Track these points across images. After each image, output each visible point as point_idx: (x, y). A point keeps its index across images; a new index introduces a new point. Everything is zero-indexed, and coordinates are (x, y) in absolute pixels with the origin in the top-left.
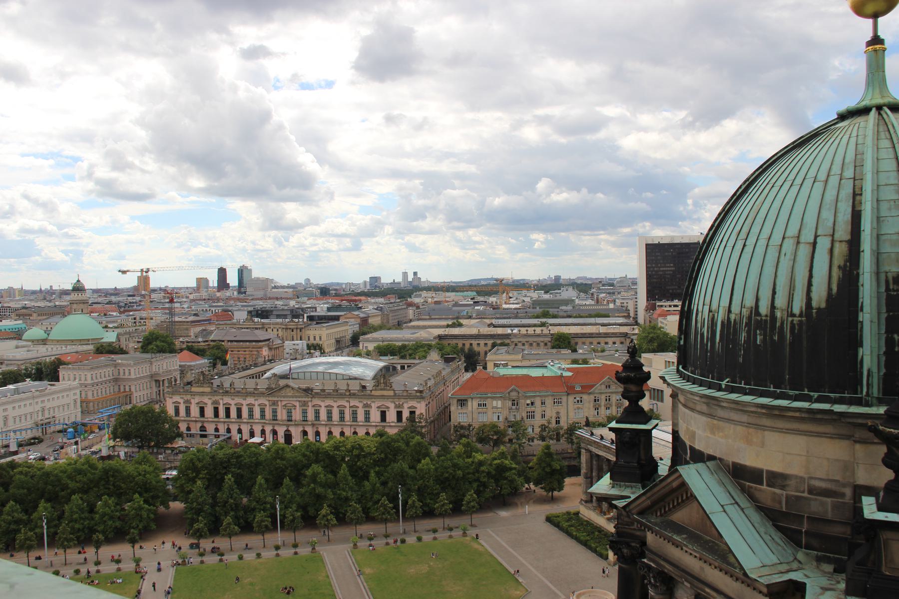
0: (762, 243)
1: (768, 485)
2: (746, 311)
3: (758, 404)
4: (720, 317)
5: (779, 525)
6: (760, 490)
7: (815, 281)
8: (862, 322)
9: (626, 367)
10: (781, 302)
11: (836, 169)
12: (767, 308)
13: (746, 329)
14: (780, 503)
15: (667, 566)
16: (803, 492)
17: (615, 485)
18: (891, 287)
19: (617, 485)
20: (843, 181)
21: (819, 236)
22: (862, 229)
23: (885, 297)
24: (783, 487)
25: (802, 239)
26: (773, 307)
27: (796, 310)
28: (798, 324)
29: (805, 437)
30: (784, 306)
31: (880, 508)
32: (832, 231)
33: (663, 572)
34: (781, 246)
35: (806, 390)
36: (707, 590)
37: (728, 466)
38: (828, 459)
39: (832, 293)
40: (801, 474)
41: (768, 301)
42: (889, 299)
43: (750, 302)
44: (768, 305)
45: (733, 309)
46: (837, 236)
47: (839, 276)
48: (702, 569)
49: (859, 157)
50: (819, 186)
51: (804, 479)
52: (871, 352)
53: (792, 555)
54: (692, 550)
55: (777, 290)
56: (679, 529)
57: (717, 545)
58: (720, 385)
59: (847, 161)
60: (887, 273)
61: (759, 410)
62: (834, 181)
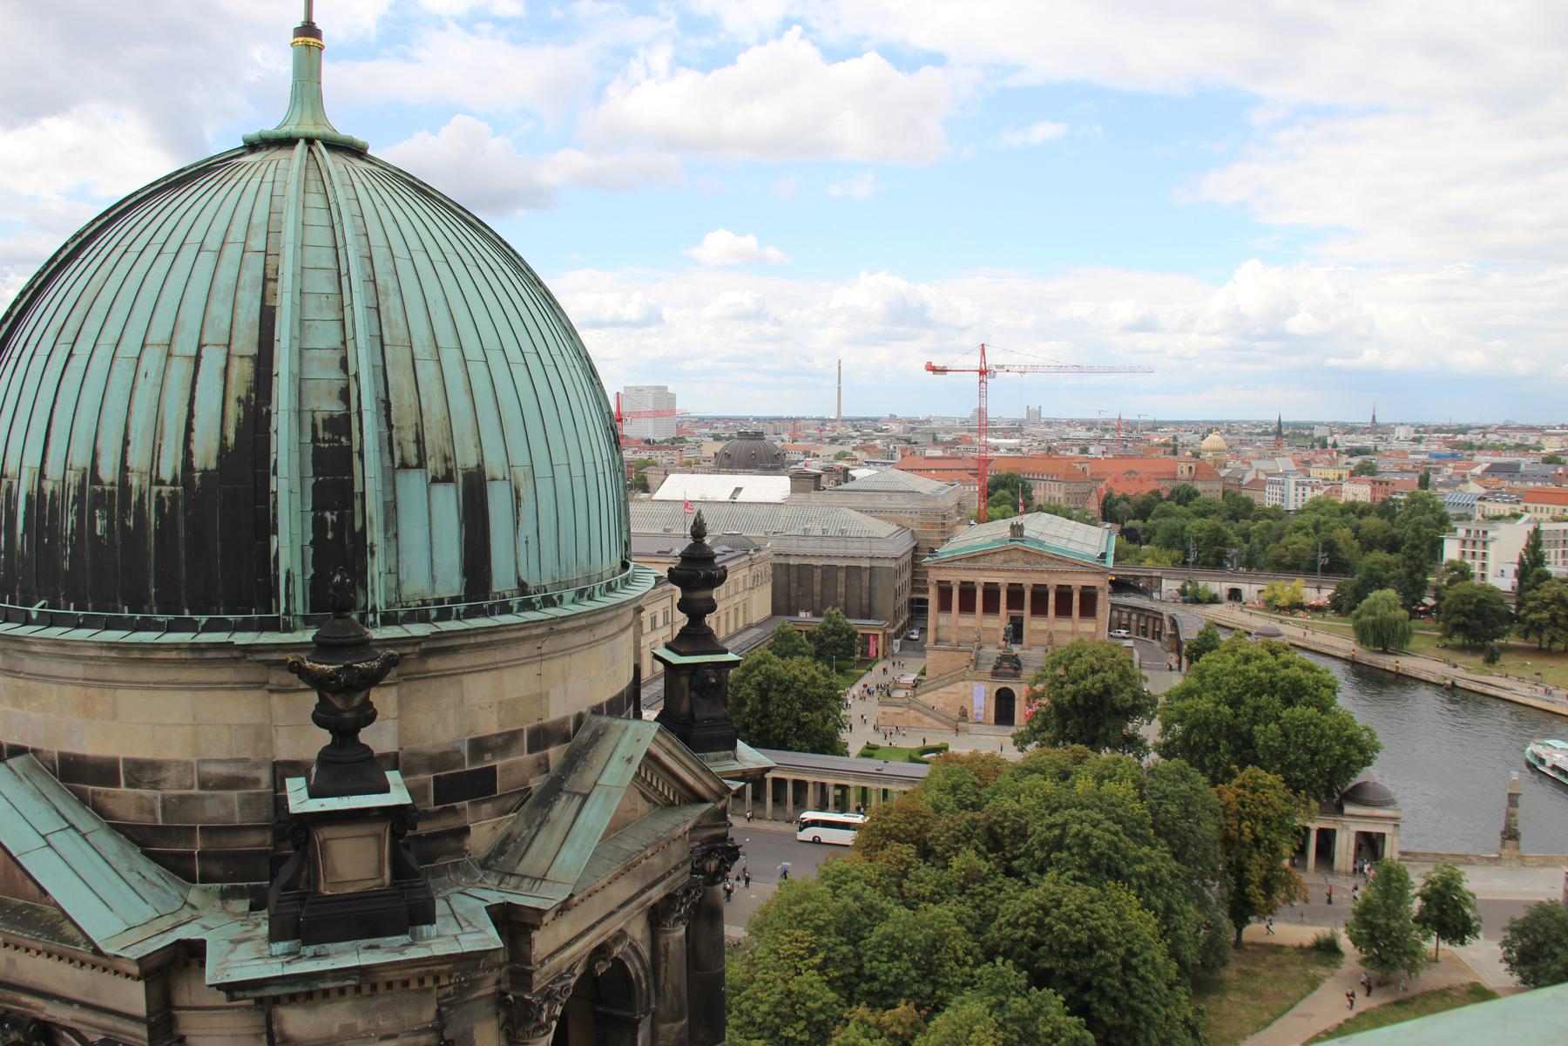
0: (104, 351)
1: (129, 785)
2: (75, 475)
4: (24, 487)
5: (151, 852)
6: (115, 796)
7: (198, 423)
8: (275, 493)
10: (138, 458)
11: (237, 233)
12: (114, 470)
13: (76, 507)
14: (152, 812)
16: (191, 787)
18: (320, 435)
20: (247, 255)
23: (311, 452)
24: (155, 785)
25: (176, 350)
26: (124, 468)
27: (166, 474)
28: (169, 498)
29: (188, 693)
30: (146, 467)
31: (314, 793)
32: (228, 338)
35: (187, 611)
37: (53, 762)
38: (229, 726)
40: (186, 758)
41: (116, 457)
43: (81, 459)
44: (115, 464)
45: (49, 471)
46: (235, 348)
49: (274, 216)
50: (207, 259)
51: (192, 764)
52: (291, 541)
53: (179, 898)
55: (131, 438)
58: (28, 613)
59: (255, 221)
60: (314, 411)
61: (104, 653)
62: (232, 253)
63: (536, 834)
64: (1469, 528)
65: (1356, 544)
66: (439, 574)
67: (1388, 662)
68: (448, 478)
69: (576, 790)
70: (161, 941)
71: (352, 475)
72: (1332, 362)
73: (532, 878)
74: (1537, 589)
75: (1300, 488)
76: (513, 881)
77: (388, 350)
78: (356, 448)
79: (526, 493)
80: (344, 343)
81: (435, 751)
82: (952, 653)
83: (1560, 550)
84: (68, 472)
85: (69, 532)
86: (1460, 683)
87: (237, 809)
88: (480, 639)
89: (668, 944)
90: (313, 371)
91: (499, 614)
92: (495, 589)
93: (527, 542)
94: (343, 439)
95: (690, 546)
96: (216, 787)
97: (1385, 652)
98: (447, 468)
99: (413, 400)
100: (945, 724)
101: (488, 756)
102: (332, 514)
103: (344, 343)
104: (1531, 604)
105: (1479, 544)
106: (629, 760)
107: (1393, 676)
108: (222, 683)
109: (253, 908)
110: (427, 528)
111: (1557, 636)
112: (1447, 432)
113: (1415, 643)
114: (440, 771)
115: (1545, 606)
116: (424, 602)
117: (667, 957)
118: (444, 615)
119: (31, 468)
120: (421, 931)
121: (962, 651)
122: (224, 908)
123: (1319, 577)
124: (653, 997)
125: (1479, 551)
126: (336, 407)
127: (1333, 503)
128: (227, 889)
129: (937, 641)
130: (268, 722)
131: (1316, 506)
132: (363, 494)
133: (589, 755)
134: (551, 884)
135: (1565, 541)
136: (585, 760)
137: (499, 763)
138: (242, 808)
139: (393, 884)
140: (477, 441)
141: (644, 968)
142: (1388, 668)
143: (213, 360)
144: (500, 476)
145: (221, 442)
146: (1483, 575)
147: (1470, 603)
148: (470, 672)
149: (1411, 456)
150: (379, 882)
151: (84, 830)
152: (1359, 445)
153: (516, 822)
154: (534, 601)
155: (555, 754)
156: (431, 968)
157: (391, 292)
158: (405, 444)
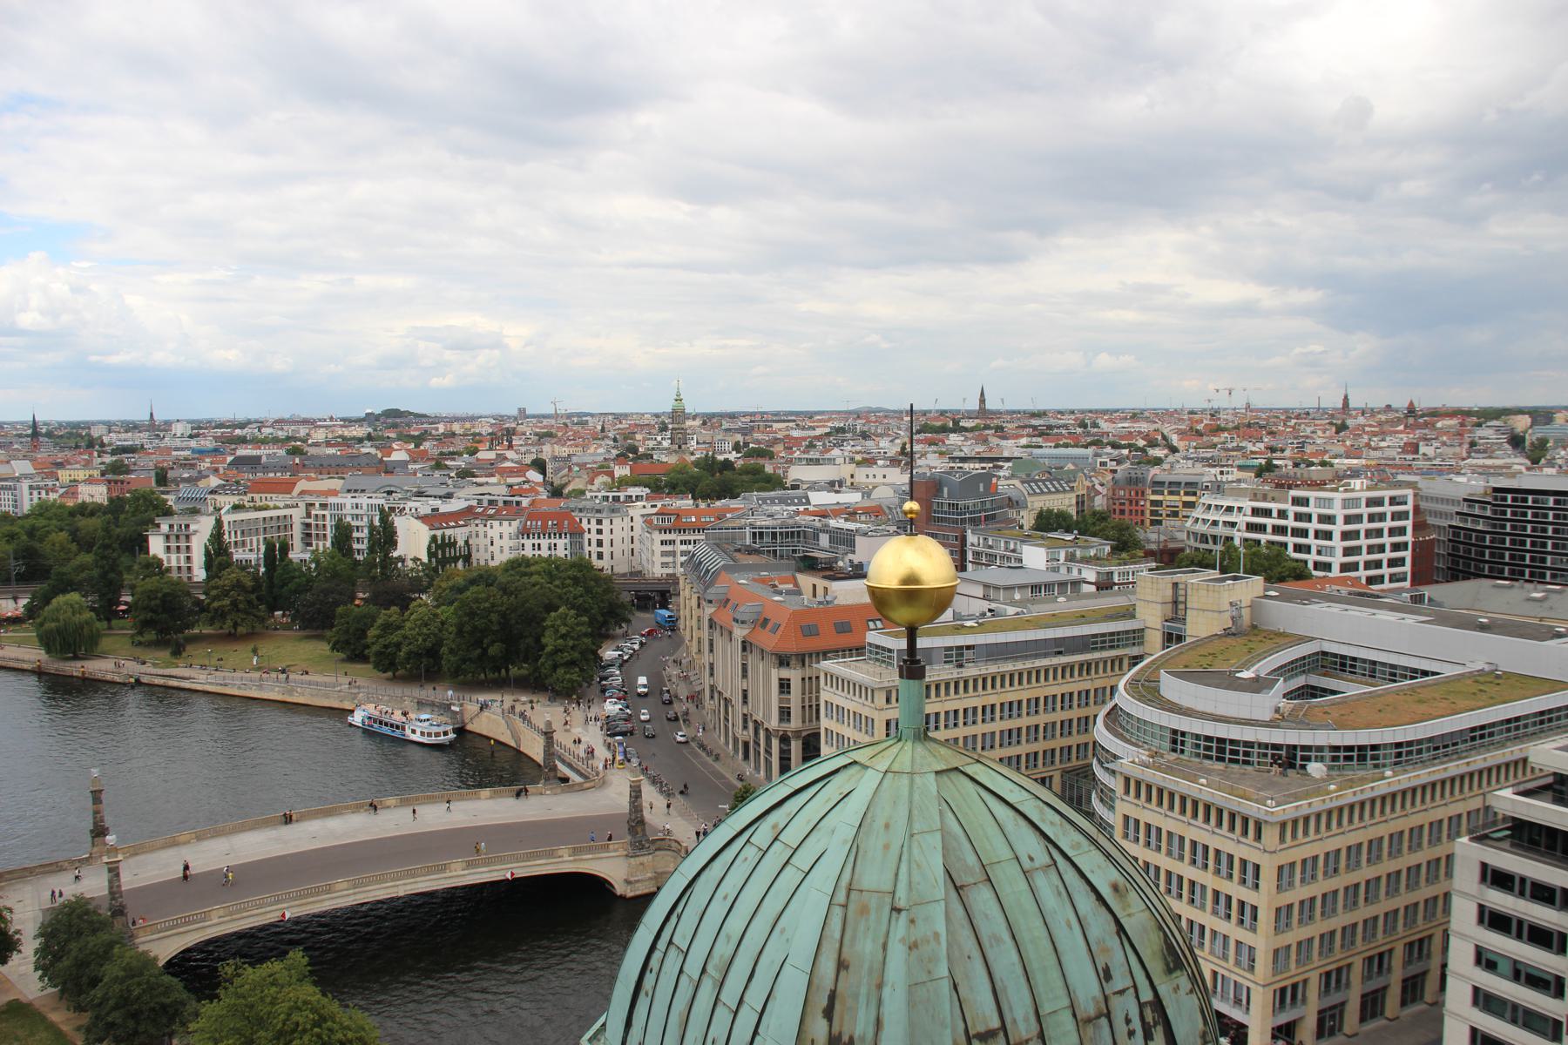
64: (171, 522)
65: (74, 547)
67: (75, 668)
72: (94, 358)
74: (220, 578)
75: (35, 493)
83: (261, 538)
86: (145, 680)
97: (76, 658)
104: (214, 592)
105: (183, 538)
107: (80, 682)
111: (239, 620)
112: (228, 427)
113: (105, 643)
115: (226, 594)
123: (14, 587)
125: (183, 545)
127: (62, 506)
131: (42, 510)
135: (265, 529)
142: (75, 674)
146: (189, 568)
147: (156, 598)
149: (174, 453)
152: (130, 443)
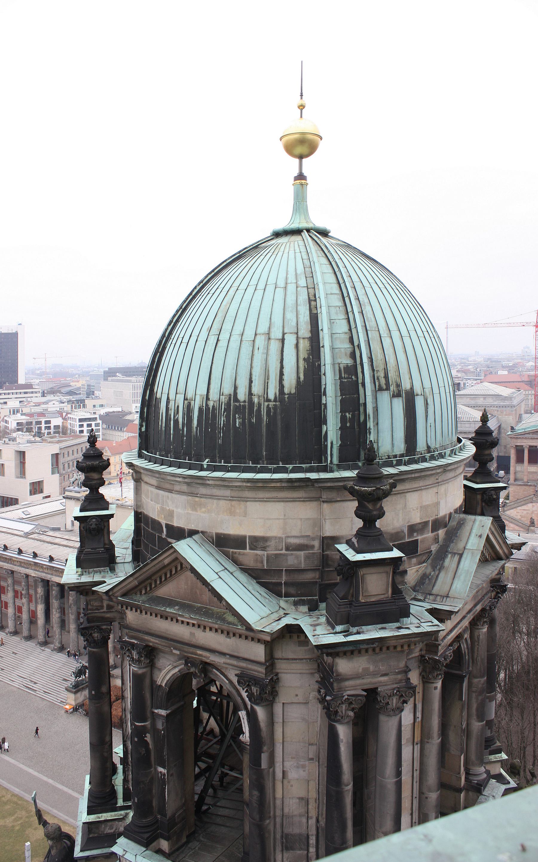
0: (235, 339)
1: (251, 549)
2: (225, 398)
3: (244, 479)
5: (261, 582)
6: (244, 554)
7: (286, 371)
8: (325, 405)
9: (86, 456)
10: (257, 389)
12: (245, 395)
14: (262, 562)
15: (152, 640)
16: (282, 550)
17: (84, 573)
18: (343, 376)
19: (86, 572)
20: (299, 289)
21: (286, 333)
22: (320, 329)
24: (264, 549)
25: (272, 336)
26: (250, 394)
27: (271, 396)
28: (273, 408)
29: (282, 503)
30: (261, 393)
32: (296, 329)
33: (147, 646)
34: (254, 341)
35: (281, 463)
36: (199, 652)
38: (301, 519)
39: (300, 381)
40: (279, 535)
42: (342, 383)
43: (228, 389)
45: (211, 397)
46: (300, 334)
47: (305, 366)
48: (192, 634)
51: (282, 538)
53: (277, 605)
54: (188, 619)
55: (253, 379)
56: (170, 603)
57: (209, 609)
58: (202, 465)
60: (339, 364)
61: (244, 484)
63: (439, 574)
66: (396, 443)
68: (398, 395)
69: (455, 551)
70: (278, 624)
71: (359, 395)
73: (441, 596)
76: (431, 597)
77: (369, 332)
78: (360, 381)
79: (430, 401)
80: (350, 330)
81: (394, 531)
82: (525, 487)
84: (221, 396)
85: (222, 426)
87: (303, 561)
88: (417, 475)
89: (479, 635)
90: (338, 345)
91: (421, 462)
92: (418, 450)
93: (431, 426)
94: (353, 377)
95: (480, 427)
96: (291, 550)
98: (398, 390)
99: (382, 357)
100: (522, 528)
101: (415, 534)
102: (349, 414)
103: (350, 330)
106: (480, 536)
108: (298, 498)
109: (310, 610)
110: (391, 420)
114: (395, 542)
116: (389, 457)
117: (479, 643)
118: (399, 463)
119: (201, 395)
120: (403, 621)
121: (530, 486)
122: (297, 610)
124: (471, 664)
126: (349, 361)
128: (297, 601)
129: (516, 480)
130: (319, 517)
132: (365, 404)
133: (458, 534)
134: (452, 599)
136: (457, 537)
137: (419, 538)
138: (305, 560)
139: (392, 597)
140: (410, 376)
141: (468, 648)
143: (290, 340)
144: (420, 393)
145: (297, 380)
148: (409, 492)
150: (386, 595)
151: (231, 571)
153: (426, 568)
154: (435, 455)
155: (441, 533)
156: (410, 639)
157: (366, 304)
158: (380, 378)
